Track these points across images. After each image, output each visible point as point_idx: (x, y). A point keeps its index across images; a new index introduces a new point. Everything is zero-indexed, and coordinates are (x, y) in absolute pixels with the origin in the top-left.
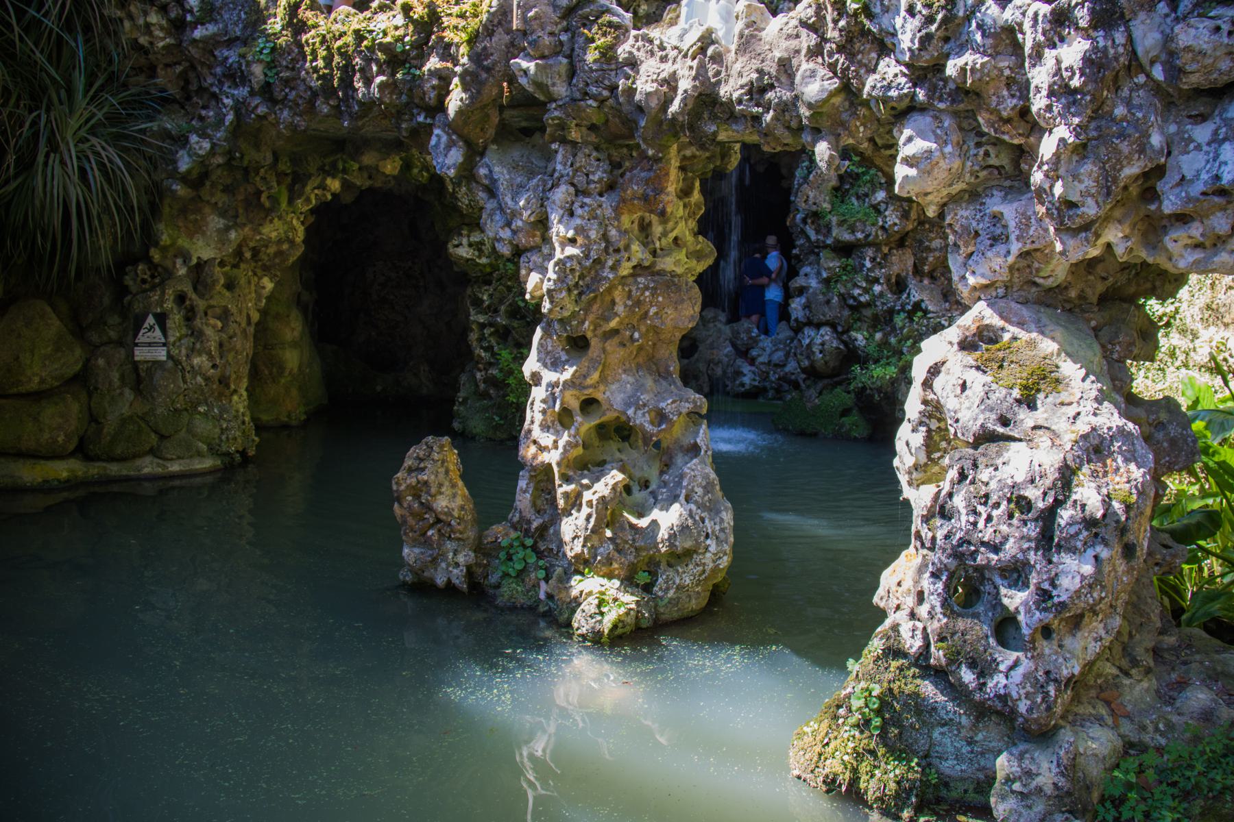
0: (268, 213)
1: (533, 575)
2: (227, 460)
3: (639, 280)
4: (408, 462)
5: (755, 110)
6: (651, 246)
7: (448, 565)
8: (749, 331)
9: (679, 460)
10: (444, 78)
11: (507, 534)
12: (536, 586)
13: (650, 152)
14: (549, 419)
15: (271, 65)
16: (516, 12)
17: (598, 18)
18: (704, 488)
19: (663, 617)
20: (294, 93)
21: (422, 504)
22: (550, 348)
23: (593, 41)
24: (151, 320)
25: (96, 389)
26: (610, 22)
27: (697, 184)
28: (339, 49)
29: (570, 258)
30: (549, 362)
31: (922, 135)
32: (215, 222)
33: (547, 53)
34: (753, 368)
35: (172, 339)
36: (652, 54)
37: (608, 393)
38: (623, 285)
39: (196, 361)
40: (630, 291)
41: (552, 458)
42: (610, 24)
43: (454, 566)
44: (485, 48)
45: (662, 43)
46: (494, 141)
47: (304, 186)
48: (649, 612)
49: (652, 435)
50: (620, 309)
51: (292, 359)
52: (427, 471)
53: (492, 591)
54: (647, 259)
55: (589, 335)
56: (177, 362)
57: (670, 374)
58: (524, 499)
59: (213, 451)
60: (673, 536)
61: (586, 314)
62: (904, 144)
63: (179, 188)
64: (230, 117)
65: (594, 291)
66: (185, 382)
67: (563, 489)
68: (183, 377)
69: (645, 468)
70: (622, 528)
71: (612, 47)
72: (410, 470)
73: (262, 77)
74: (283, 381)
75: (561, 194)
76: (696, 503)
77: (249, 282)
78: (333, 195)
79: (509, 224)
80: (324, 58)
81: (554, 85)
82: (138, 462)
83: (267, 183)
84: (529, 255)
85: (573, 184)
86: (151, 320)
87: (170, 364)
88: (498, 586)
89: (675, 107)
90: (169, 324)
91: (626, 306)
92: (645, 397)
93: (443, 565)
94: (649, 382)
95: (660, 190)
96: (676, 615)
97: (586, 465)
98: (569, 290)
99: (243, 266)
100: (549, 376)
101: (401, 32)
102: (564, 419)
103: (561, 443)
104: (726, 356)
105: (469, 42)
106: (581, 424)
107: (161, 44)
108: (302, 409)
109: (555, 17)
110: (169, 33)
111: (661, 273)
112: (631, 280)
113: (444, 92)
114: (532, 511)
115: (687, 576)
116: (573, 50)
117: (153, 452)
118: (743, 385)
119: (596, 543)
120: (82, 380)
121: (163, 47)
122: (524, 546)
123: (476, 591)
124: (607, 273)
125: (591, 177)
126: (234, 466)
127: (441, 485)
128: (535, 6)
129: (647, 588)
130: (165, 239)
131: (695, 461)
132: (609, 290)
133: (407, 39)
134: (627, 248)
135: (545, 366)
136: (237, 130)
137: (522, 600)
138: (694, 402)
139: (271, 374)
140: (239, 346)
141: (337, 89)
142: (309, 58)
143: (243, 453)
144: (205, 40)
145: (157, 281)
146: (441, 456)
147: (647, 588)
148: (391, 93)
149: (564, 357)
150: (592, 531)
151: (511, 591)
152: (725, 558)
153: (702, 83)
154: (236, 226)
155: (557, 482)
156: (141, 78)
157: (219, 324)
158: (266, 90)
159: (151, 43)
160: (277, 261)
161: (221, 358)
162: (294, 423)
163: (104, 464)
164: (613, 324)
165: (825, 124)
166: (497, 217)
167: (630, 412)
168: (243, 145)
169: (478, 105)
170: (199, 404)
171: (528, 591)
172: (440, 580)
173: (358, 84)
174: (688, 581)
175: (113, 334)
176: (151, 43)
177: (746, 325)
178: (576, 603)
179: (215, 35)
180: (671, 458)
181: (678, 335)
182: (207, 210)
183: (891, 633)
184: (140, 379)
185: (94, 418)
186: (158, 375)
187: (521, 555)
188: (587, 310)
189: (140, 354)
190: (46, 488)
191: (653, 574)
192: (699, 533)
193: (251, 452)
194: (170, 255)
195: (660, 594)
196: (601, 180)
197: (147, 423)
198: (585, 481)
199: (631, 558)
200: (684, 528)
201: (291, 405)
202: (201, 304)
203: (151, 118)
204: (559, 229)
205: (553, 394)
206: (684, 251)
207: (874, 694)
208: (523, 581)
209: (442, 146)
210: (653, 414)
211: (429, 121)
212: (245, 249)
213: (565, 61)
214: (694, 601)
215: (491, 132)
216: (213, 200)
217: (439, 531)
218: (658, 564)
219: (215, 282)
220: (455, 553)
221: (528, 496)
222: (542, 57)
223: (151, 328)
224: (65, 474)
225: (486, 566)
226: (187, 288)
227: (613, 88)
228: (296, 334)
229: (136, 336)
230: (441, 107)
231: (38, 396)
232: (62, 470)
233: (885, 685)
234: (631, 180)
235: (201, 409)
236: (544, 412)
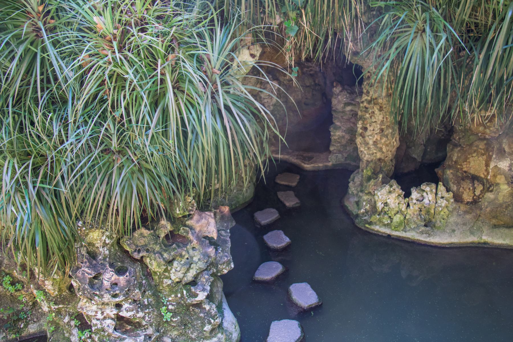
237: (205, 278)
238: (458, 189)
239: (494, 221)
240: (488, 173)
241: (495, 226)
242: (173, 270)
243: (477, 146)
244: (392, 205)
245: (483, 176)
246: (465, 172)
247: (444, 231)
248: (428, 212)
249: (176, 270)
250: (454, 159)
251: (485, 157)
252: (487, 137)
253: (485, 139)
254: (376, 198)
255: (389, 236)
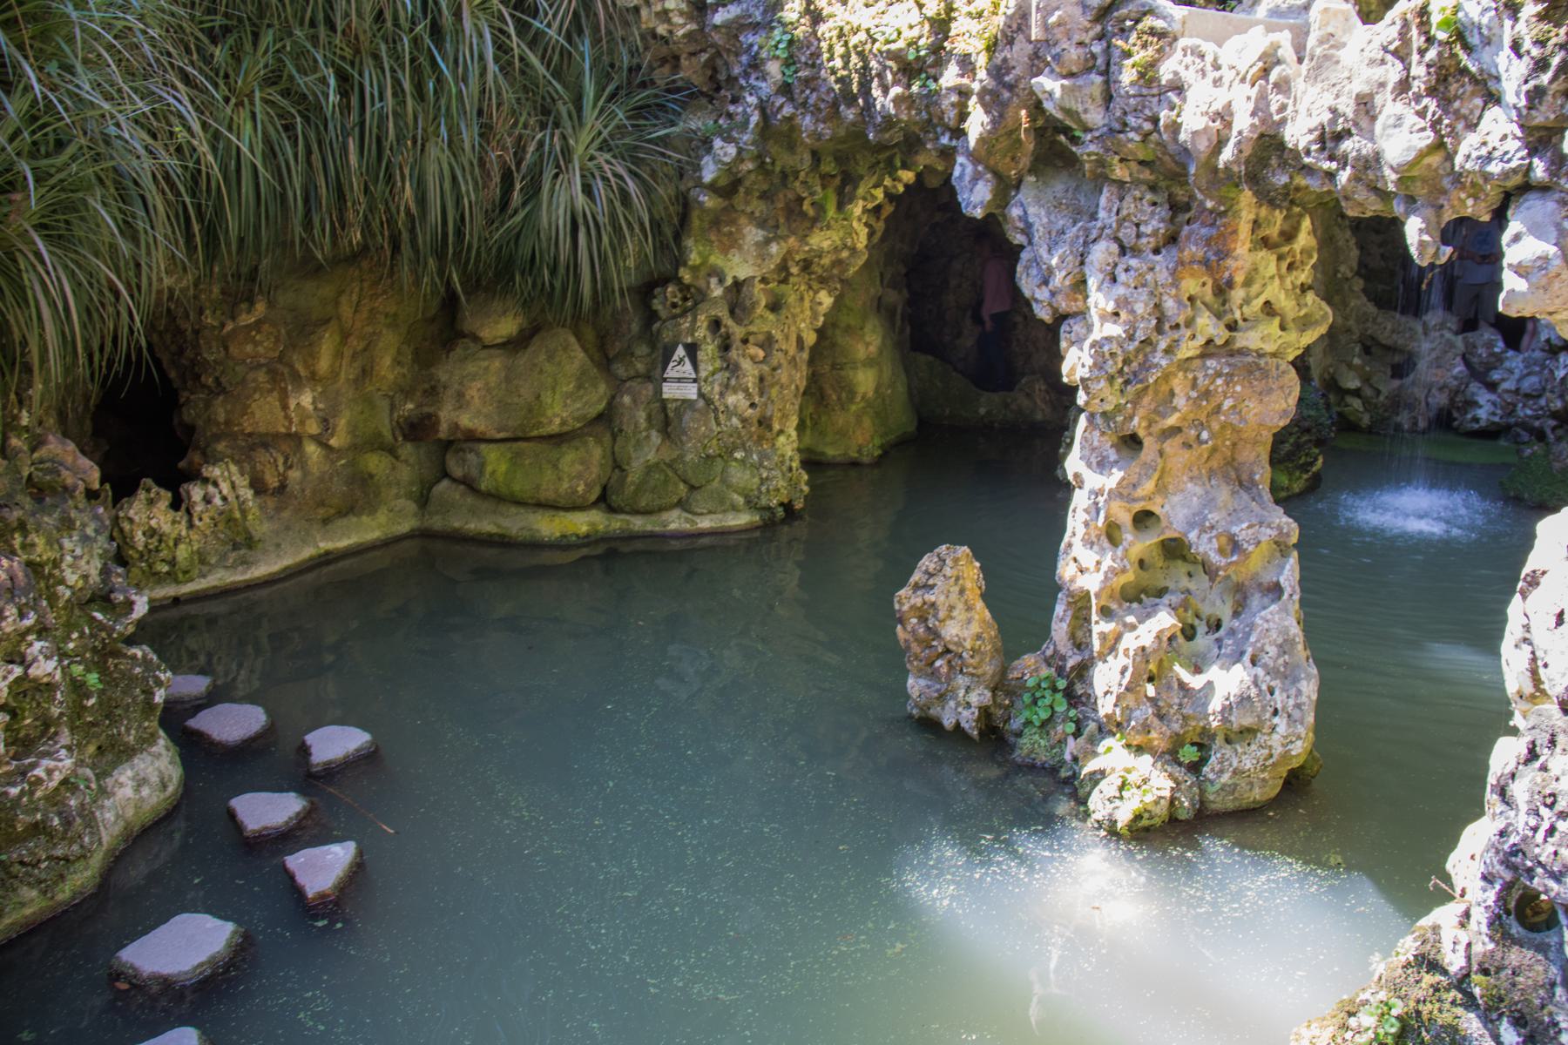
0: (816, 221)
1: (1060, 728)
2: (767, 515)
3: (1209, 363)
4: (917, 577)
5: (1326, 165)
6: (1228, 317)
7: (958, 705)
8: (1490, 345)
9: (1255, 601)
10: (964, 93)
11: (1036, 670)
12: (1062, 742)
13: (1209, 204)
14: (1093, 534)
15: (789, 62)
16: (1035, 18)
17: (1137, 21)
18: (1280, 646)
19: (1213, 806)
20: (814, 95)
21: (928, 628)
22: (1096, 443)
23: (1128, 55)
24: (680, 352)
25: (621, 431)
26: (1152, 29)
27: (1306, 223)
28: (855, 47)
29: (1108, 339)
30: (1094, 460)
31: (1536, 230)
32: (753, 234)
33: (1075, 69)
34: (1493, 397)
35: (703, 374)
36: (1203, 73)
37: (1167, 507)
38: (1186, 371)
39: (731, 399)
40: (1195, 379)
41: (1091, 583)
42: (1152, 32)
43: (964, 706)
44: (1005, 60)
45: (1215, 59)
46: (1030, 171)
47: (856, 188)
48: (1192, 800)
49: (1218, 569)
50: (1180, 401)
51: (865, 381)
52: (936, 590)
53: (1012, 739)
54: (1220, 335)
55: (1141, 433)
56: (709, 402)
57: (1254, 484)
58: (1060, 630)
59: (751, 504)
60: (1227, 709)
61: (1134, 408)
62: (1508, 245)
63: (708, 200)
64: (755, 118)
65: (1141, 381)
66: (719, 424)
67: (1101, 627)
68: (716, 418)
69: (1218, 602)
70: (1169, 687)
71: (1153, 64)
72: (917, 587)
73: (779, 76)
74: (854, 408)
75: (1102, 252)
76: (1265, 666)
77: (802, 299)
78: (906, 186)
79: (1046, 282)
80: (842, 57)
81: (1086, 111)
82: (665, 516)
83: (809, 188)
84: (1071, 321)
85: (1116, 239)
86: (680, 352)
87: (701, 403)
88: (1019, 734)
89: (1227, 154)
90: (701, 355)
91: (1189, 398)
92: (1213, 517)
93: (952, 704)
94: (1223, 494)
95: (1224, 254)
96: (1230, 806)
97: (1138, 596)
98: (1111, 379)
99: (792, 279)
100: (1093, 480)
101: (915, 32)
102: (1112, 534)
103: (1104, 567)
104: (1456, 378)
105: (988, 49)
106: (1131, 544)
107: (680, 33)
108: (877, 441)
109: (1084, 21)
110: (690, 17)
111: (1243, 352)
112: (1197, 362)
113: (963, 116)
114: (1069, 645)
115: (1247, 758)
116: (1108, 64)
117: (682, 504)
118: (1476, 420)
119: (1132, 704)
120: (606, 420)
121: (684, 36)
122: (1055, 690)
123: (994, 735)
124: (1160, 359)
125: (1142, 228)
126: (778, 522)
127: (952, 608)
128: (1058, 8)
129: (1195, 768)
130: (694, 258)
131: (1274, 607)
132: (1166, 377)
133: (922, 42)
134: (1189, 323)
135: (1089, 465)
136: (766, 129)
137: (1043, 757)
138: (1279, 528)
139: (839, 399)
140: (784, 379)
141: (853, 94)
142: (826, 56)
143: (788, 507)
144: (727, 25)
145: (689, 304)
146: (955, 572)
147: (1195, 768)
148: (909, 108)
149: (1113, 456)
150: (1127, 689)
151: (1032, 745)
152: (1299, 743)
153: (1263, 122)
154: (777, 238)
155: (1094, 617)
156: (666, 69)
157: (761, 354)
158: (785, 89)
159: (671, 32)
160: (835, 271)
161: (761, 395)
162: (866, 460)
163: (628, 517)
164: (1172, 421)
165: (1420, 191)
166: (1034, 271)
167: (1193, 536)
168: (774, 148)
169: (1002, 132)
170: (735, 449)
171: (1053, 747)
173: (876, 92)
175: (640, 367)
176: (671, 32)
177: (1486, 336)
178: (1097, 777)
179: (738, 17)
180: (1245, 598)
181: (1267, 437)
182: (743, 220)
183: (1429, 935)
184: (667, 419)
185: (618, 466)
186: (687, 417)
187: (1047, 701)
188: (1136, 401)
189: (670, 391)
190: (562, 544)
192: (1264, 707)
193: (799, 505)
194: (703, 273)
195: (1211, 776)
196: (1155, 233)
197: (675, 472)
198: (1130, 619)
199: (1176, 727)
200: (1244, 700)
201: (859, 437)
202: (738, 331)
203: (673, 124)
204: (1099, 300)
205: (1096, 504)
206: (1277, 321)
207: (1394, 1012)
208: (1048, 733)
209: (967, 178)
210: (1224, 540)
211: (954, 143)
212: (790, 263)
213: (1098, 79)
215: (1025, 162)
216: (749, 210)
218: (1213, 737)
219: (754, 305)
220: (968, 689)
221: (1065, 625)
222: (1071, 75)
223: (681, 361)
224: (584, 529)
225: (1007, 708)
226: (722, 312)
227: (1155, 120)
228: (872, 349)
229: (664, 369)
230: (959, 133)
231: (559, 439)
232: (581, 523)
233: (1412, 1004)
234: (1188, 238)
235: (738, 455)
236: (1086, 524)
237: (119, 575)
238: (253, 468)
239: (322, 512)
240: (291, 422)
241: (326, 521)
242: (69, 559)
243: (255, 380)
244: (166, 528)
245: (283, 430)
246: (250, 435)
247: (265, 551)
248: (230, 520)
249: (75, 558)
250: (222, 417)
251: (275, 394)
252: (262, 361)
253: (260, 366)
254: (126, 526)
255: (176, 601)
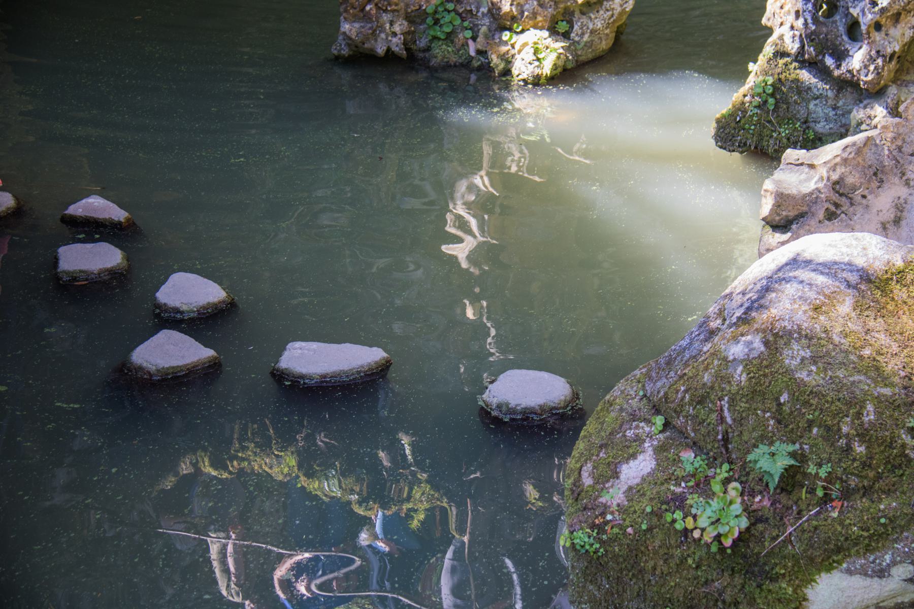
1: (461, 36)
7: (387, 35)
12: (465, 45)
19: (581, 58)
88: (428, 49)
96: (590, 56)
137: (454, 59)
147: (566, 36)
151: (442, 53)
172: (381, 50)
174: (599, 26)
183: (778, 41)
191: (571, 24)
195: (577, 39)
207: (769, 83)
208: (452, 42)
214: (604, 42)
217: (376, 5)
218: (572, 14)
225: (414, 32)
233: (776, 76)
